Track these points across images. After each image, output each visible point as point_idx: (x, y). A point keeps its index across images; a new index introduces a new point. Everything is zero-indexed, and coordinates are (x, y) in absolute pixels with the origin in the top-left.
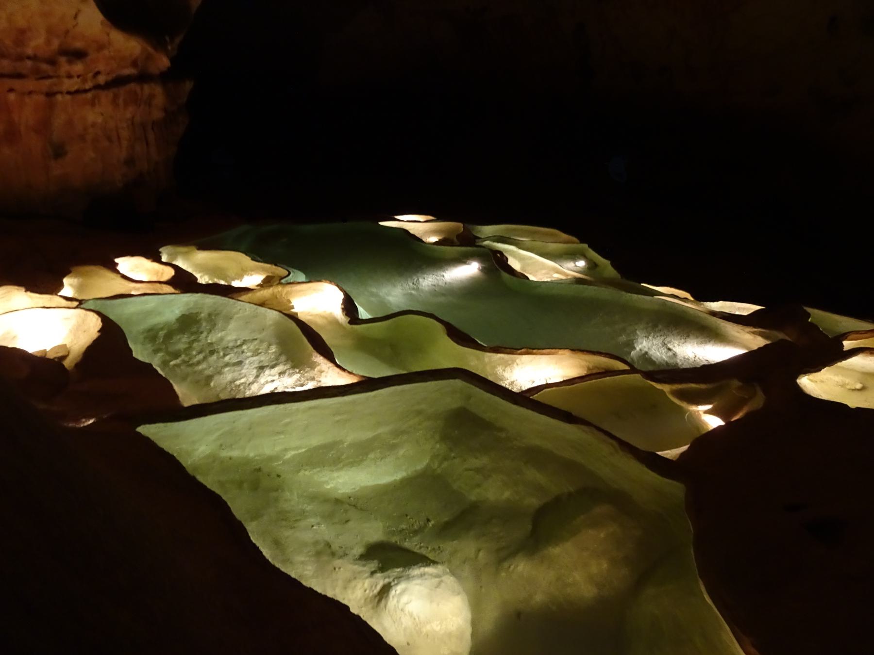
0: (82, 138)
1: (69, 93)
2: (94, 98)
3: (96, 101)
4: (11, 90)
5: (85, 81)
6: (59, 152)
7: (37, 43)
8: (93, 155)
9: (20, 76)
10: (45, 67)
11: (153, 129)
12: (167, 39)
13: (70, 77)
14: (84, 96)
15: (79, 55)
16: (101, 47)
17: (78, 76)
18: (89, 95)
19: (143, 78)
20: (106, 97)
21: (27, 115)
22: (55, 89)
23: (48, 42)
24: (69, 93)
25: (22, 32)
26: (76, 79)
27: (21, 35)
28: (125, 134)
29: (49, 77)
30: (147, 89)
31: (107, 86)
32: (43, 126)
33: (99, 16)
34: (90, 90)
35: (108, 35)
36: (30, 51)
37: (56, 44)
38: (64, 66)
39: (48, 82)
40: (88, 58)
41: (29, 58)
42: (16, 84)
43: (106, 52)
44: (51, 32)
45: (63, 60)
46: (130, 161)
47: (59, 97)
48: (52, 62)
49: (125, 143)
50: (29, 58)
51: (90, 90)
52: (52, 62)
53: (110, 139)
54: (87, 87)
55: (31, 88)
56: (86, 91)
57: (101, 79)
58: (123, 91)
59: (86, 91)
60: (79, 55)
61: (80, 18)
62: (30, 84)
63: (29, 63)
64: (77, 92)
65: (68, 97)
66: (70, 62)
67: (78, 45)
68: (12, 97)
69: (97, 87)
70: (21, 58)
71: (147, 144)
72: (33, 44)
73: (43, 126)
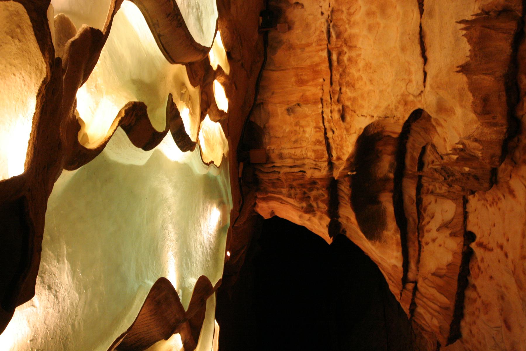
0: (297, 124)
1: (323, 112)
2: (319, 128)
3: (318, 130)
4: (324, 80)
5: (329, 122)
6: (290, 111)
7: (348, 93)
8: (287, 130)
9: (331, 84)
10: (336, 97)
11: (301, 171)
12: (355, 173)
13: (331, 112)
14: (321, 121)
15: (343, 118)
16: (347, 130)
17: (331, 117)
18: (321, 125)
19: (331, 165)
20: (320, 136)
21: (312, 90)
22: (325, 104)
23: (349, 99)
24: (323, 112)
25: (353, 86)
26: (330, 115)
27: (351, 85)
28: (298, 152)
29: (331, 99)
30: (324, 165)
31: (327, 138)
32: (305, 101)
33: (363, 127)
34: (324, 126)
35: (355, 133)
36: (344, 89)
37: (348, 103)
38: (337, 107)
39: (329, 98)
40: (341, 122)
41: (340, 89)
42: (328, 81)
43: (345, 133)
44: (354, 100)
45: (340, 107)
46: (281, 156)
47: (320, 106)
48: (339, 101)
49: (293, 151)
50: (340, 89)
51: (324, 126)
52: (339, 101)
53: (295, 142)
54: (326, 124)
55: (325, 90)
56: (323, 123)
57: (330, 134)
58: (323, 148)
59: (323, 123)
60: (343, 118)
61: (363, 118)
62: (327, 88)
63: (338, 89)
64: (323, 118)
65: (320, 111)
66: (339, 111)
67: (348, 118)
68: (321, 80)
69: (325, 133)
70: (340, 85)
71: (291, 167)
72: (347, 90)
73: (305, 101)
